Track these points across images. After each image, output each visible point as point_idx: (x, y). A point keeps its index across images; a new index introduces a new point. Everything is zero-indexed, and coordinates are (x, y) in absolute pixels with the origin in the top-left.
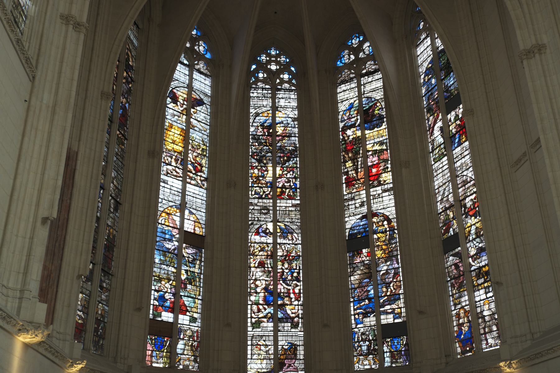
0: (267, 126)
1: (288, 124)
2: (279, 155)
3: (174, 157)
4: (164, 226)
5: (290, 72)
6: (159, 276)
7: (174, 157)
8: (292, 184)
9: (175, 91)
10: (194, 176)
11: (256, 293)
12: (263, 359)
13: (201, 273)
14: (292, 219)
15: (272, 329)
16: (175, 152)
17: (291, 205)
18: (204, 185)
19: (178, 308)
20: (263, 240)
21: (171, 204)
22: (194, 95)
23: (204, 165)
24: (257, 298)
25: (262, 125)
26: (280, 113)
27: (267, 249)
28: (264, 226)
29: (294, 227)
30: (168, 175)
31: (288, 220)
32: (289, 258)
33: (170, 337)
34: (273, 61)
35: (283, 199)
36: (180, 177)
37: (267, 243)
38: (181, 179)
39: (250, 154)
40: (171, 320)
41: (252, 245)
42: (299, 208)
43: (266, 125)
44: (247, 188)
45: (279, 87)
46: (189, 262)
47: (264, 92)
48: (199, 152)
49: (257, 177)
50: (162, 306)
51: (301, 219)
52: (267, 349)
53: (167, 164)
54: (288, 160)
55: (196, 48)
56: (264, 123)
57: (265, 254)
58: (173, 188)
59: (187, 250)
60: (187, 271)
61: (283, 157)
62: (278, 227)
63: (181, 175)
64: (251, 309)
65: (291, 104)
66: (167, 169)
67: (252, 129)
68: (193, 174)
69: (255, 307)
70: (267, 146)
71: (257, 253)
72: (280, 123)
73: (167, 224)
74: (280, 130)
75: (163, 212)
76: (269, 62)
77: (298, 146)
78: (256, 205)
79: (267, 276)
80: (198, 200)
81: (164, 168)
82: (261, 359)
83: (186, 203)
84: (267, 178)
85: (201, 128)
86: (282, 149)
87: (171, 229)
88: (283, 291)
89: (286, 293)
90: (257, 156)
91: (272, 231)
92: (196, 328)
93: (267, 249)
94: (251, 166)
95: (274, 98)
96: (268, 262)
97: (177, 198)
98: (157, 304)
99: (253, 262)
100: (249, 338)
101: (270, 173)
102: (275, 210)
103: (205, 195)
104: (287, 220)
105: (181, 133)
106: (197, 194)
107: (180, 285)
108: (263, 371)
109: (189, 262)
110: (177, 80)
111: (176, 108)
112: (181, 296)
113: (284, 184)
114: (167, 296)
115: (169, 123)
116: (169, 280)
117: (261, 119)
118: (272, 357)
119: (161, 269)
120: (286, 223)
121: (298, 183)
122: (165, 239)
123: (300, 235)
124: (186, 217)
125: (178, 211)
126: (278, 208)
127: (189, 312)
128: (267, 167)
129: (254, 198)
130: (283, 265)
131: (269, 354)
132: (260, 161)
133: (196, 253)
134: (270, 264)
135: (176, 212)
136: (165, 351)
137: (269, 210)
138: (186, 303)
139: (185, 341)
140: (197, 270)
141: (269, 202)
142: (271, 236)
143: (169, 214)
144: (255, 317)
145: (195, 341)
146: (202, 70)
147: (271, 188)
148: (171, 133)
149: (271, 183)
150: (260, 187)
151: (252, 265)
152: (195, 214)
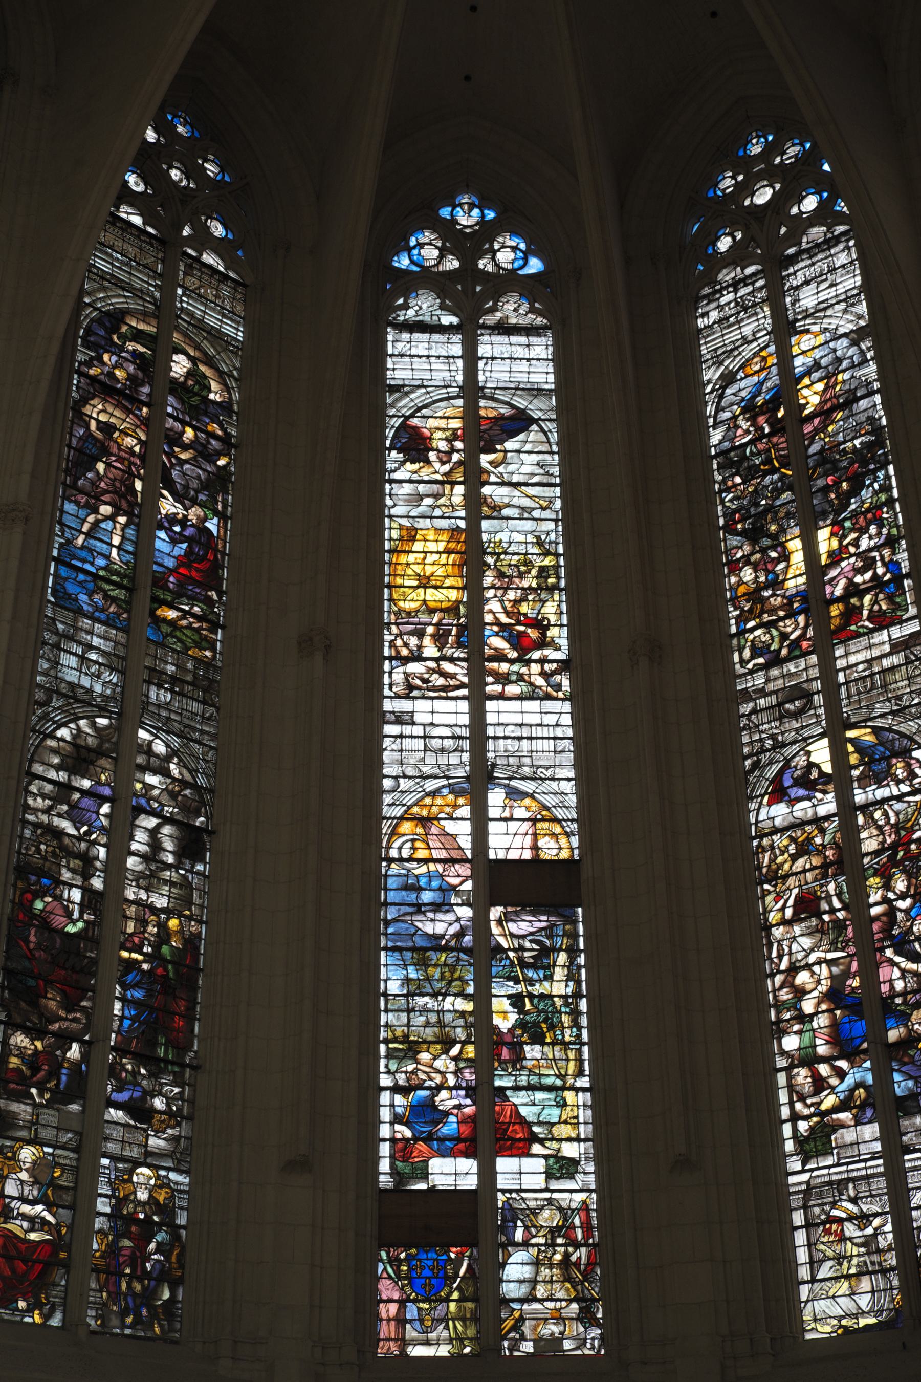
0: (766, 402)
1: (839, 360)
2: (820, 483)
3: (430, 630)
4: (414, 865)
5: (819, 183)
6: (405, 1039)
7: (430, 630)
8: (880, 571)
9: (415, 421)
10: (515, 668)
11: (803, 1018)
12: (859, 1275)
13: (577, 995)
14: (899, 698)
15: (877, 1146)
16: (432, 611)
18: (558, 687)
19: (494, 1134)
20: (803, 809)
21: (431, 785)
22: (487, 409)
23: (553, 619)
24: (807, 1036)
25: (750, 409)
26: (807, 337)
27: (818, 840)
28: (801, 761)
30: (415, 693)
32: (907, 851)
34: (760, 176)
35: (857, 635)
36: (462, 686)
37: (817, 821)
38: (465, 692)
39: (721, 522)
40: (471, 1182)
41: (766, 842)
43: (760, 400)
45: (791, 251)
46: (523, 964)
48: (530, 581)
49: (754, 596)
50: (429, 1139)
52: (869, 1231)
53: (405, 660)
54: (855, 491)
55: (481, 264)
56: (754, 397)
57: (816, 861)
58: (436, 732)
59: (513, 927)
60: (516, 1000)
61: (837, 483)
62: (850, 748)
63: (465, 680)
64: (791, 1087)
65: (841, 289)
66: (407, 675)
67: (716, 436)
68: (512, 662)
69: (802, 1075)
70: (774, 471)
71: (786, 866)
72: (808, 373)
73: (422, 854)
74: (811, 396)
75: (402, 818)
76: (746, 188)
79: (834, 947)
80: (539, 745)
81: (395, 676)
82: (848, 1277)
83: (494, 765)
84: (790, 584)
85: (527, 502)
87: (440, 867)
88: (899, 985)
89: (914, 992)
90: (743, 520)
91: (827, 768)
92: (579, 1197)
93: (818, 840)
94: (729, 563)
96: (831, 887)
97: (454, 759)
98: (408, 1134)
99: (777, 907)
100: (796, 1201)
101: (798, 558)
102: (831, 689)
103: (567, 720)
105: (452, 545)
106: (536, 725)
107: (495, 1050)
108: (863, 1322)
109: (523, 964)
110: (419, 387)
111: (425, 474)
112: (503, 1089)
113: (850, 581)
114: (445, 1101)
115: (401, 527)
116: (447, 1043)
117: (744, 386)
118: (891, 1260)
119: (409, 1011)
120: (879, 723)
121: (903, 557)
122: (419, 908)
124: (493, 813)
125: (461, 801)
126: (841, 678)
127: (542, 1142)
128: (783, 545)
129: (751, 672)
130: (887, 886)
131: (879, 1251)
132: (753, 535)
133: (549, 931)
134: (839, 895)
135: (456, 807)
136: (456, 1295)
137: (808, 696)
138: (523, 1111)
139: (534, 1251)
140: (559, 987)
142: (831, 787)
143: (424, 821)
144: (806, 1112)
145: (577, 1246)
146: (513, 321)
147: (804, 611)
148: (412, 558)
149: (803, 596)
150: (768, 625)
151: (773, 917)
152: (532, 796)
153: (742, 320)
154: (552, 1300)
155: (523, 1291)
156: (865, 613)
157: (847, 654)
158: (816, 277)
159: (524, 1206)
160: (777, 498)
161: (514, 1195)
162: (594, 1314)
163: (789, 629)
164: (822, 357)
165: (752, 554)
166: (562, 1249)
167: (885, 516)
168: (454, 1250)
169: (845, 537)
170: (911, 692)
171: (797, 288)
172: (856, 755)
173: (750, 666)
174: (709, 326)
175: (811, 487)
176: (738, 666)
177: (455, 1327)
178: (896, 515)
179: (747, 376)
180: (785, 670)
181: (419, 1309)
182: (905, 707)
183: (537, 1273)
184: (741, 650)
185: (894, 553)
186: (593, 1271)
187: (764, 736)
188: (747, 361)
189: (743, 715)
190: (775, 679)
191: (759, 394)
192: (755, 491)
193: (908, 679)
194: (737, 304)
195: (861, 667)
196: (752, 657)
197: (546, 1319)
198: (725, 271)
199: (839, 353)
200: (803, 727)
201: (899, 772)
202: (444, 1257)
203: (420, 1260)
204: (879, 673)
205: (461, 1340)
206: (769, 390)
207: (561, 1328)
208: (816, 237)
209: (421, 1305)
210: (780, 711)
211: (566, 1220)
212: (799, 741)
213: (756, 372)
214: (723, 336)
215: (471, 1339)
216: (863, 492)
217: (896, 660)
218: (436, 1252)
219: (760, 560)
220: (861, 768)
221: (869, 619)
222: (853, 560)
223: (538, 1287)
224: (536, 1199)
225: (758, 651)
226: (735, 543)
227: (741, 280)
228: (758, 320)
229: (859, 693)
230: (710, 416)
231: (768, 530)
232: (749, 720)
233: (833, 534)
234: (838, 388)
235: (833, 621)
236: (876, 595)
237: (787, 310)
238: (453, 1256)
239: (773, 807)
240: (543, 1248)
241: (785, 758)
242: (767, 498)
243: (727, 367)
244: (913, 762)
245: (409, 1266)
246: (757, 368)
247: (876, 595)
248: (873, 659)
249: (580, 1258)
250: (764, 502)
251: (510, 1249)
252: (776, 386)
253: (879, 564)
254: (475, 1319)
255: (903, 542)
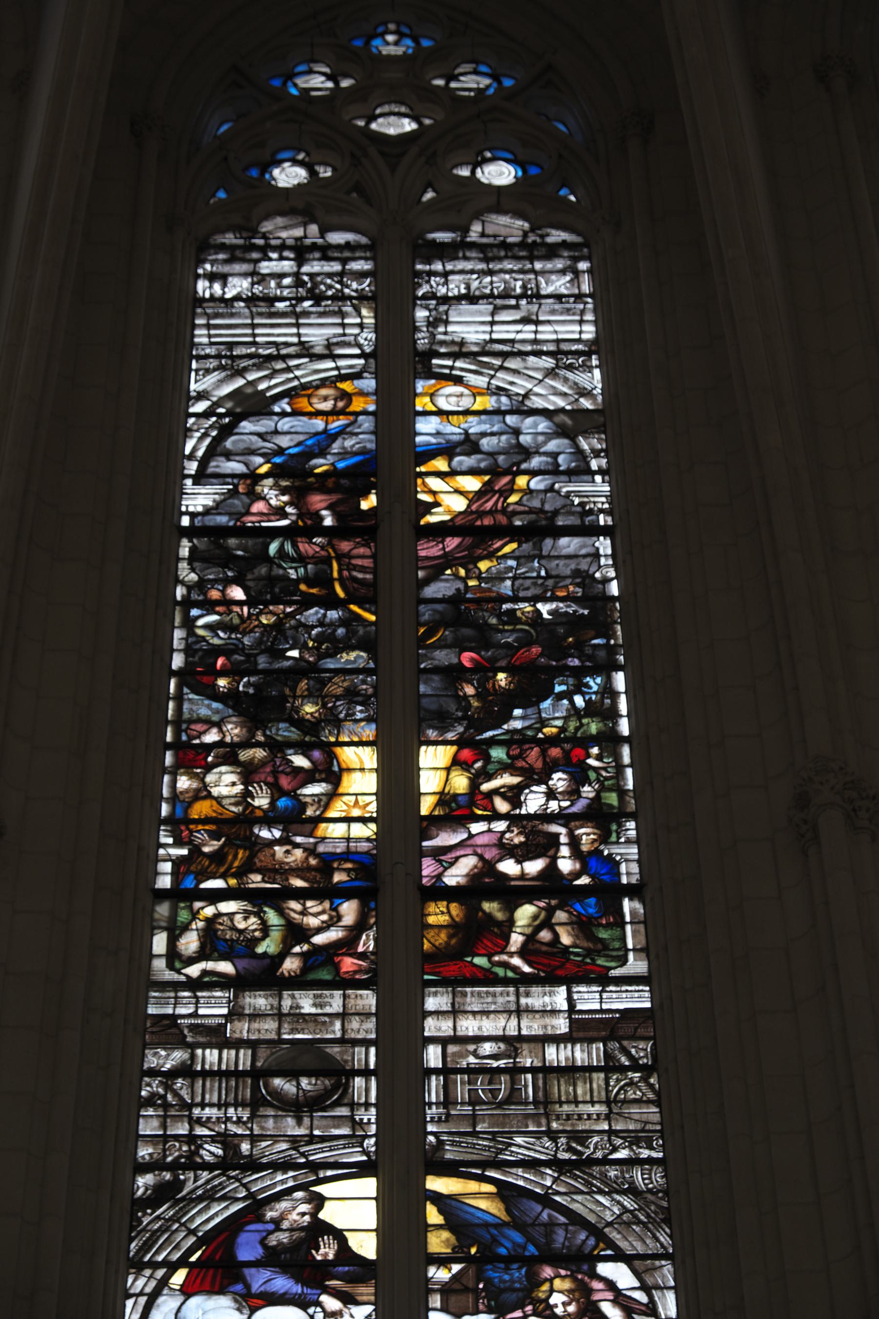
1: (527, 453)
2: (443, 657)
8: (566, 865)
14: (582, 1137)
17: (562, 1025)
25: (293, 472)
28: (296, 1212)
29: (606, 1207)
31: (543, 1150)
35: (488, 979)
39: (178, 661)
42: (642, 1050)
43: (321, 465)
44: (135, 906)
47: (314, 267)
49: (236, 827)
51: (668, 1131)
54: (532, 689)
56: (309, 454)
61: (484, 672)
62: (433, 1216)
65: (546, 333)
67: (198, 499)
74: (449, 496)
77: (614, 589)
78: (215, 1036)
86: (464, 617)
91: (366, 1246)
95: (392, 301)
104: (521, 1146)
120: (519, 1178)
123: (667, 1273)
126: (433, 1056)
128: (329, 750)
129: (194, 985)
137: (340, 1075)
141: (347, 1015)
142: (366, 1291)
150: (258, 900)
153: (306, 314)
156: (516, 940)
157: (455, 1012)
158: (491, 296)
160: (333, 654)
163: (313, 922)
164: (484, 434)
165: (247, 744)
167: (591, 762)
169: (490, 777)
170: (611, 1132)
171: (445, 300)
172: (445, 1235)
173: (194, 971)
174: (222, 300)
175: (419, 659)
176: (159, 964)
178: (620, 768)
179: (295, 413)
180: (287, 1003)
182: (591, 1162)
184: (175, 932)
185: (604, 838)
187: (200, 1131)
188: (304, 387)
189: (153, 1073)
190: (256, 1016)
191: (323, 453)
192: (279, 626)
193: (608, 1102)
194: (299, 283)
195: (487, 1048)
196: (201, 955)
198: (280, 221)
199: (525, 439)
200: (311, 1139)
201: (557, 1299)
204: (532, 1070)
206: (345, 454)
208: (503, 232)
210: (255, 1089)
212: (297, 1167)
213: (318, 413)
214: (253, 326)
216: (546, 704)
217: (580, 1055)
219: (263, 763)
220: (456, 1268)
221: (523, 953)
222: (500, 826)
225: (222, 946)
226: (204, 712)
227: (314, 247)
228: (343, 325)
229: (474, 1101)
230: (191, 457)
231: (297, 710)
232: (168, 1088)
233: (456, 762)
234: (513, 498)
235: (430, 934)
236: (550, 911)
237: (416, 329)
239: (194, 1301)
241: (251, 1195)
242: (303, 647)
243: (251, 383)
244: (597, 1285)
246: (327, 406)
247: (550, 911)
248: (520, 1038)
250: (295, 653)
252: (363, 452)
253: (565, 851)
255: (631, 825)
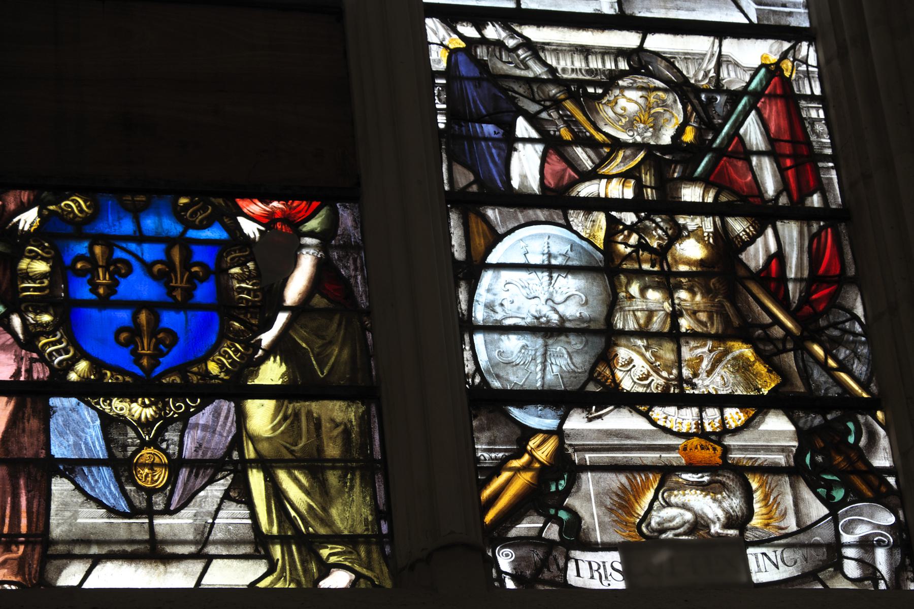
33: (319, 178)
92: (752, 54)
136: (272, 373)
154: (682, 401)
155: (561, 364)
159: (537, 70)
161: (492, 32)
162: (862, 456)
166: (708, 225)
168: (256, 208)
177: (276, 493)
181: (109, 423)
183: (613, 304)
186: (835, 303)
197: (666, 472)
202: (214, 233)
203: (110, 242)
205: (309, 544)
207: (735, 503)
209: (118, 406)
211: (708, 126)
215: (350, 541)
218: (178, 214)
223: (623, 353)
224: (585, 51)
238: (250, 228)
240: (629, 218)
245: (56, 261)
249: (779, 257)
251: (492, 213)
254: (362, 462)
